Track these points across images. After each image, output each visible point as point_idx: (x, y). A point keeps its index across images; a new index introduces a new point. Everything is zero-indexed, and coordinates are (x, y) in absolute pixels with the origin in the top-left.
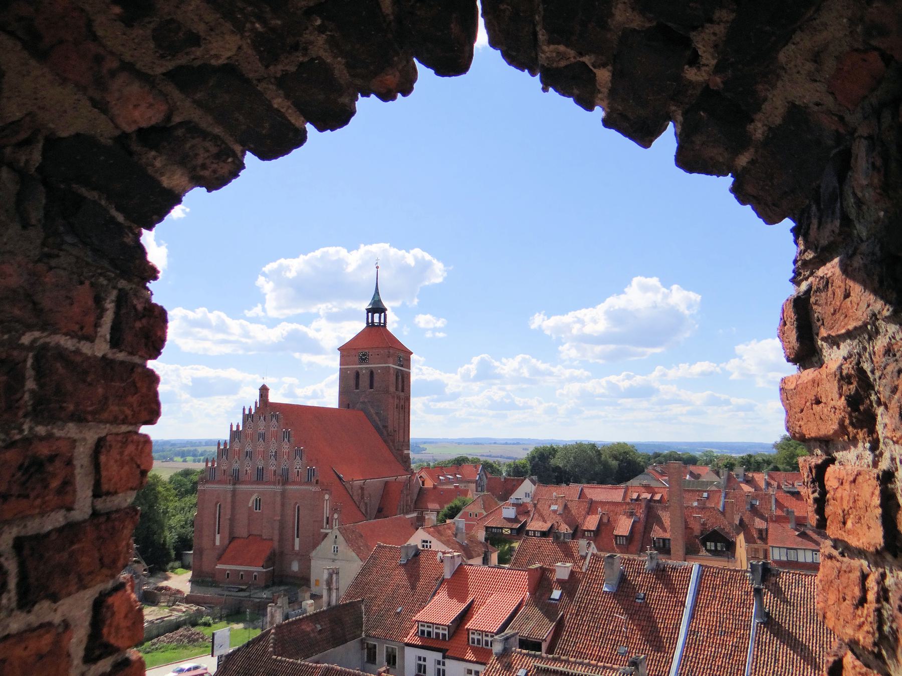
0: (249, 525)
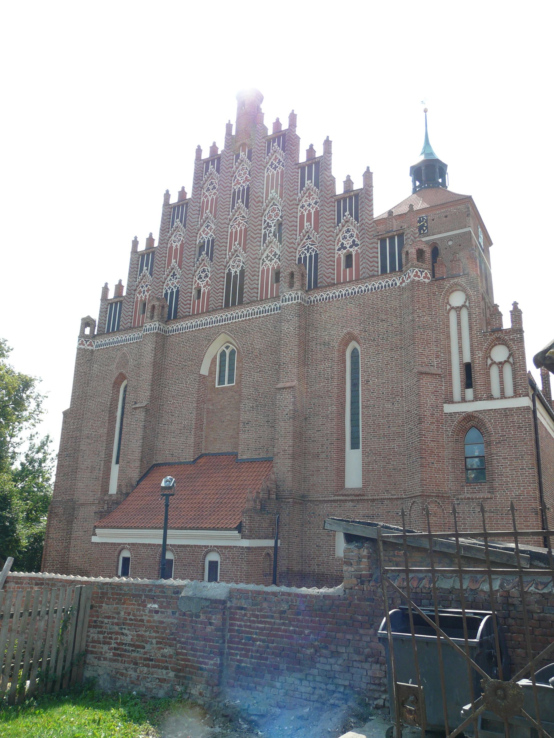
0: (199, 427)
